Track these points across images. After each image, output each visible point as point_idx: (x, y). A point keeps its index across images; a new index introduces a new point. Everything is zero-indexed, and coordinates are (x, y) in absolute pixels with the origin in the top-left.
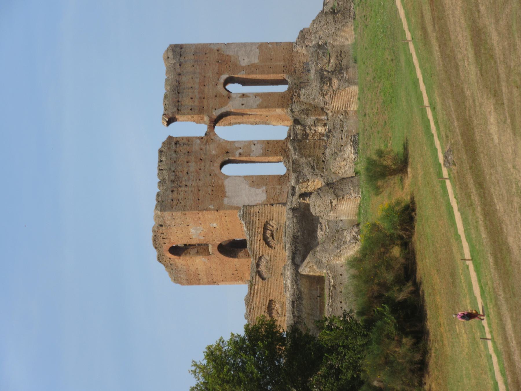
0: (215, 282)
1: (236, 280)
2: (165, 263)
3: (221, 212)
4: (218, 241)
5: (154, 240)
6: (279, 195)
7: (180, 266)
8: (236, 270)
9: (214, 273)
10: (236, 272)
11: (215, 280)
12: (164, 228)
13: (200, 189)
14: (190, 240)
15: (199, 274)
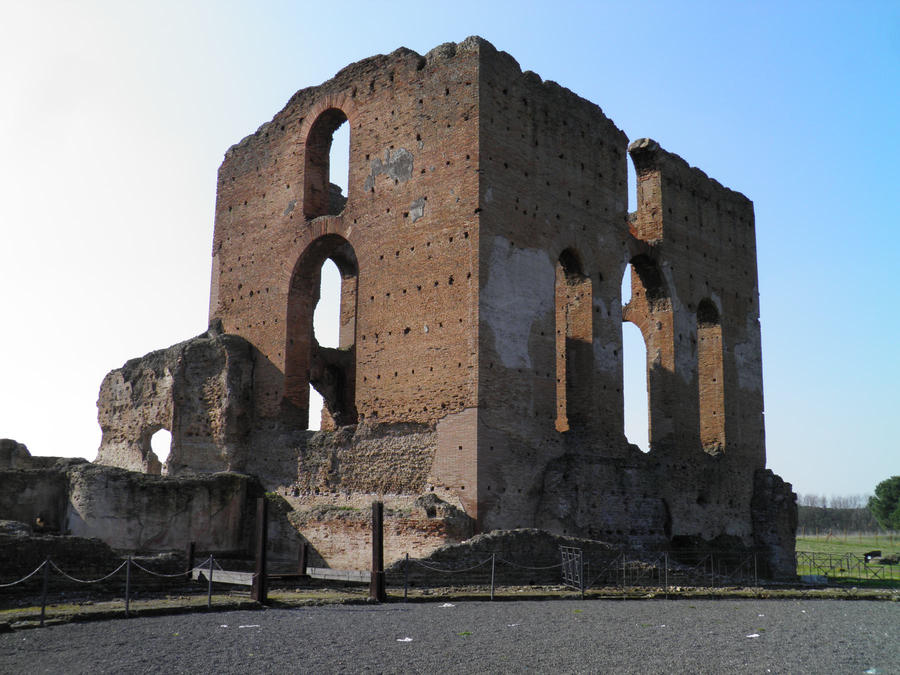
0: (221, 247)
1: (221, 296)
2: (288, 112)
3: (473, 224)
4: (354, 232)
5: (367, 62)
6: (512, 407)
7: (274, 152)
8: (252, 293)
9: (250, 237)
10: (245, 291)
11: (226, 244)
12: (412, 74)
13: (530, 177)
14: (364, 156)
15: (246, 203)
